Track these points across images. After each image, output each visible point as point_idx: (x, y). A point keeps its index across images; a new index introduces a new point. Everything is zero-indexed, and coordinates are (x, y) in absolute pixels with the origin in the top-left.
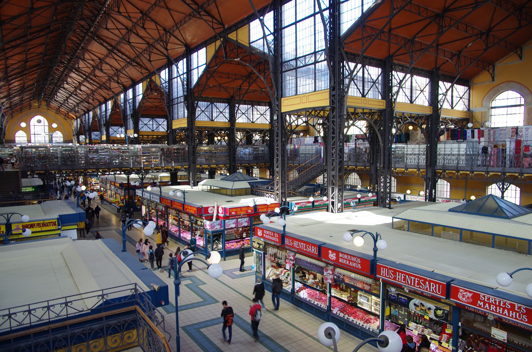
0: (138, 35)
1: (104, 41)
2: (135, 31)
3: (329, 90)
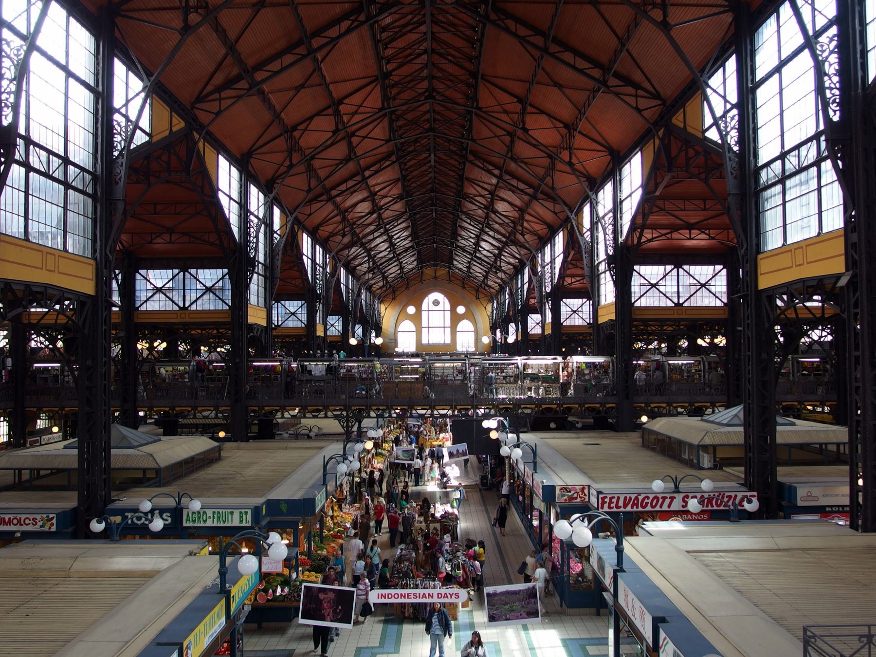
1: (485, 161)
3: (842, 232)
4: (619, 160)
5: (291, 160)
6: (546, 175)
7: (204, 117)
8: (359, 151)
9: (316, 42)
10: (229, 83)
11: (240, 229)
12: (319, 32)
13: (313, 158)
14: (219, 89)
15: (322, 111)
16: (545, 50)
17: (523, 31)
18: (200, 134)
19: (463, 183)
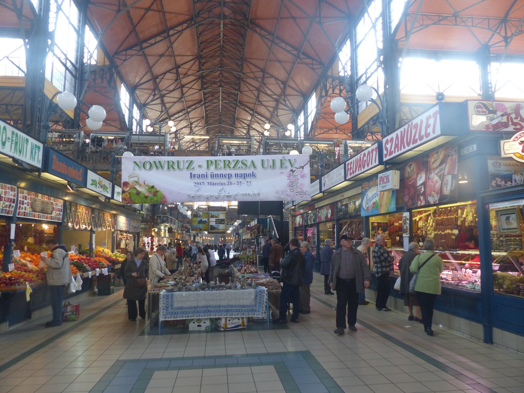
2: (263, 91)
4: (306, 97)
5: (155, 93)
7: (118, 62)
8: (185, 95)
9: (171, 32)
10: (130, 48)
11: (129, 121)
12: (172, 28)
13: (164, 96)
14: (126, 50)
15: (171, 70)
18: (115, 70)
19: (234, 120)
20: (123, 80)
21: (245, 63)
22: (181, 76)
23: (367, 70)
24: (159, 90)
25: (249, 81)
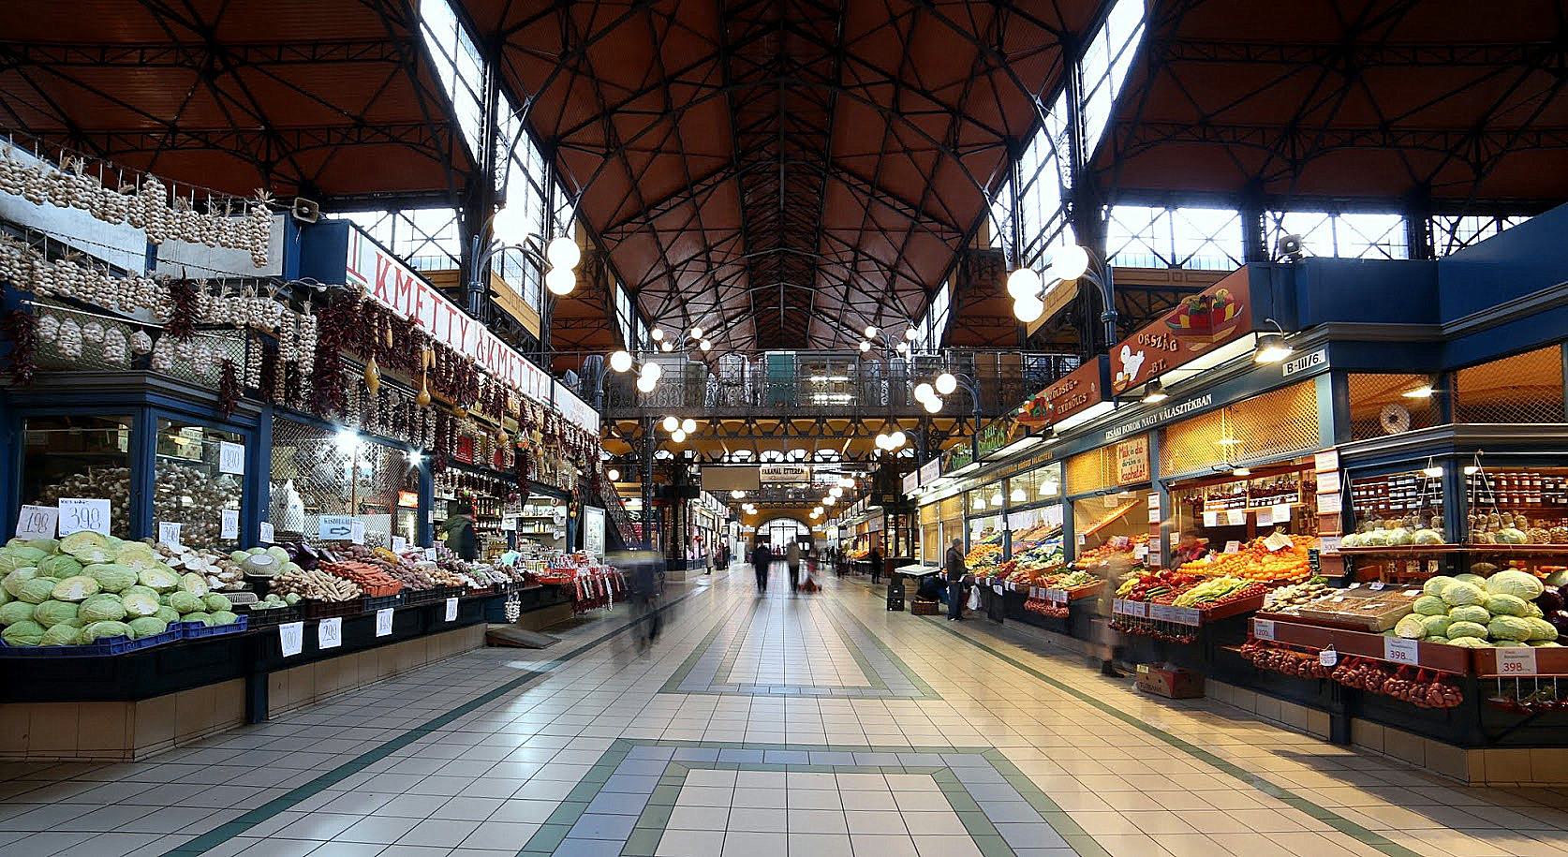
0: (861, 290)
4: (931, 294)
6: (875, 319)
9: (697, 189)
10: (628, 219)
12: (699, 181)
14: (623, 222)
16: (872, 194)
17: (854, 181)
20: (619, 278)
21: (823, 239)
22: (715, 266)
23: (1043, 231)
24: (678, 292)
25: (829, 268)
